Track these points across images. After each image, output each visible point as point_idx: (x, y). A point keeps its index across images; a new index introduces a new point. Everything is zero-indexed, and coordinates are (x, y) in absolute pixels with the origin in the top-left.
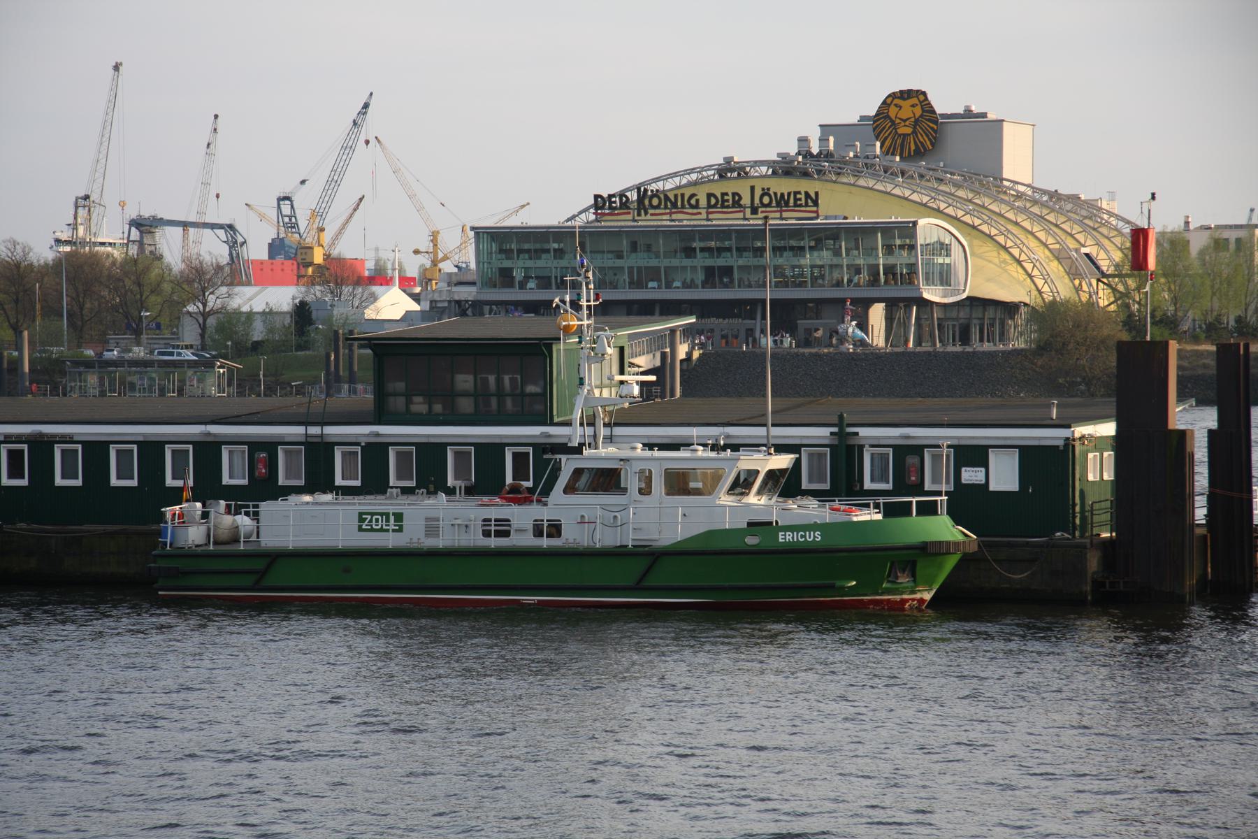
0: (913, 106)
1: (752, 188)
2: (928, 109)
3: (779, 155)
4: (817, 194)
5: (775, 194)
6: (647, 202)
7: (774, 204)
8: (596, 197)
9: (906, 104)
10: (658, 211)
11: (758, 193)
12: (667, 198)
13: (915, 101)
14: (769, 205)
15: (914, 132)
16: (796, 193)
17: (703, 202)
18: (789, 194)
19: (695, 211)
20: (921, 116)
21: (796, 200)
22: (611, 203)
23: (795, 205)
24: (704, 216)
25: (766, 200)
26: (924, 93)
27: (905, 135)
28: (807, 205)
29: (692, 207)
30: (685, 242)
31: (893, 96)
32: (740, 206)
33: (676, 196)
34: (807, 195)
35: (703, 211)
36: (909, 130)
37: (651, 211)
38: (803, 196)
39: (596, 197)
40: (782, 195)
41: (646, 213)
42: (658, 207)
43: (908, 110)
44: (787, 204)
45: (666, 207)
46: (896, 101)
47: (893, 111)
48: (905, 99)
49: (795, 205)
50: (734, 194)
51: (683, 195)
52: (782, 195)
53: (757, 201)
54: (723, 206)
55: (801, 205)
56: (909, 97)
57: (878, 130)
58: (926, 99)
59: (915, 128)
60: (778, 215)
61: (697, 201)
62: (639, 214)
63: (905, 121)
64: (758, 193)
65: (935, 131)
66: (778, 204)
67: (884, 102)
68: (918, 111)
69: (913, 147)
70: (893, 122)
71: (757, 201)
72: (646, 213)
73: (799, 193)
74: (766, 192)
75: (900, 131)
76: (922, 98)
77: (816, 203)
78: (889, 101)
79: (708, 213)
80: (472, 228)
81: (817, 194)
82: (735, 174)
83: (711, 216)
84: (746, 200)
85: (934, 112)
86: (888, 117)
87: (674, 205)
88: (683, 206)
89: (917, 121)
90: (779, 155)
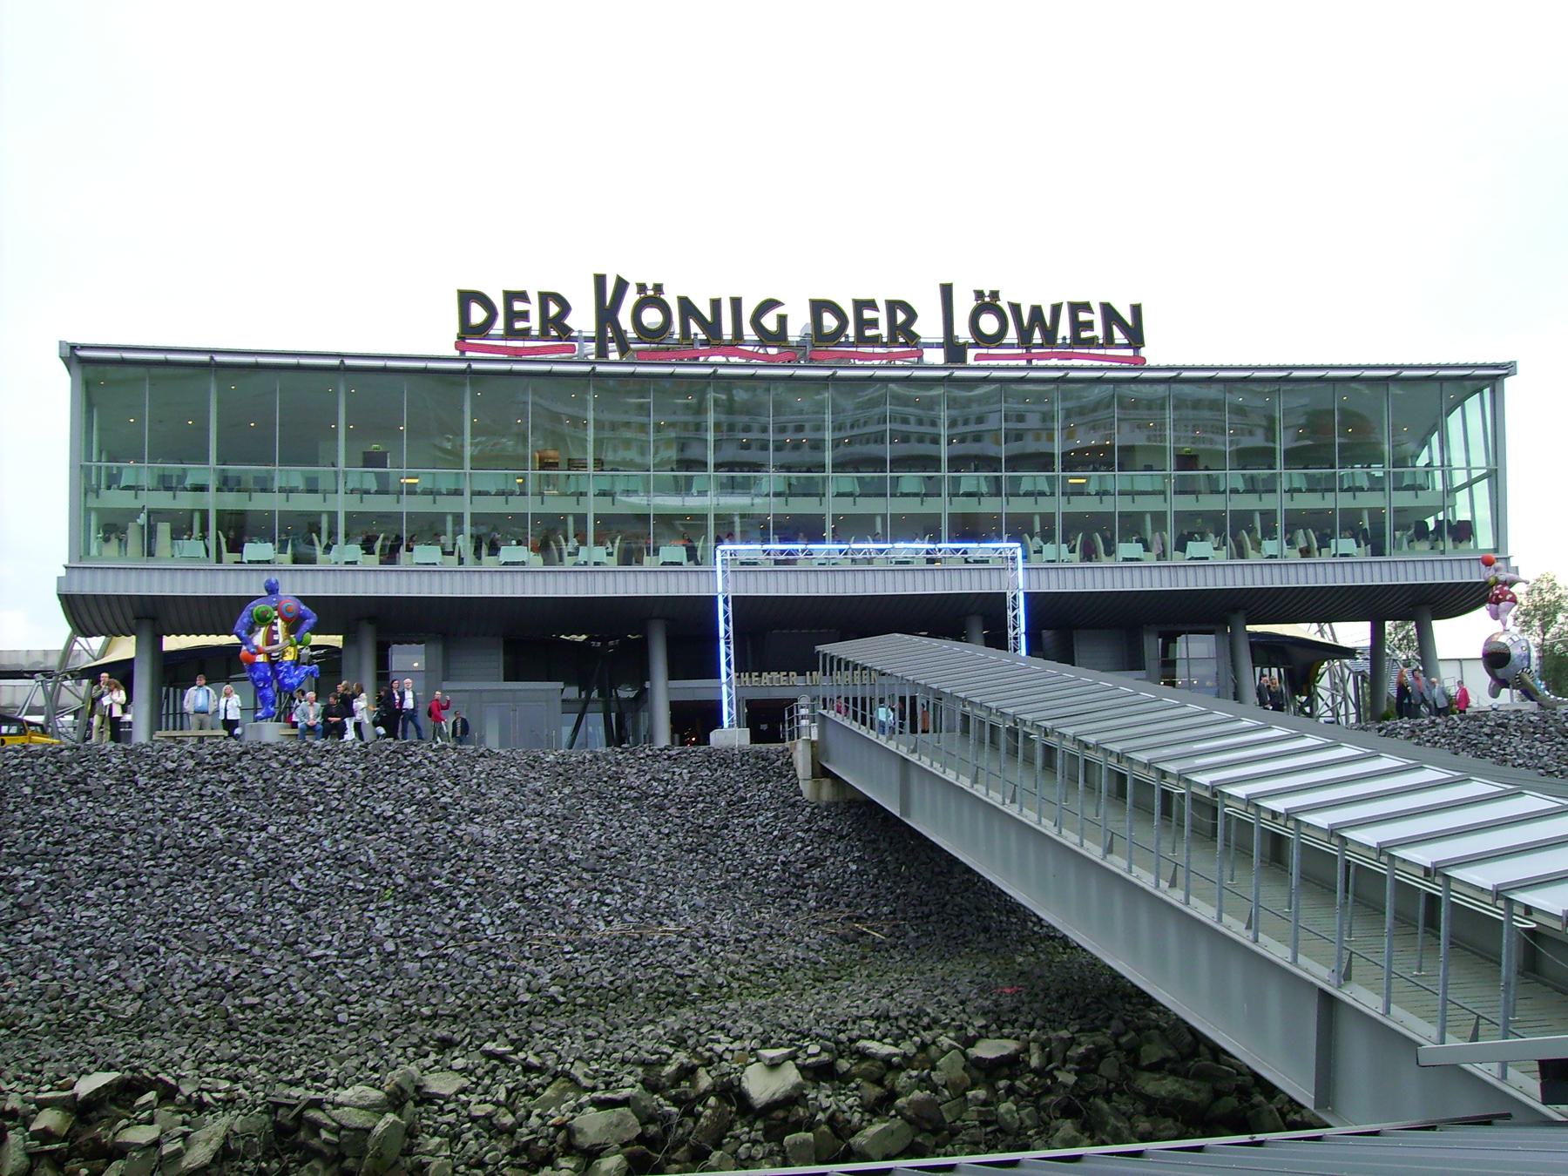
1: (947, 291)
4: (1136, 310)
5: (1016, 308)
6: (625, 318)
7: (1012, 335)
8: (467, 298)
16: (1076, 308)
18: (1056, 309)
21: (1077, 326)
25: (989, 324)
33: (716, 304)
34: (1109, 313)
38: (1097, 318)
39: (467, 298)
40: (1036, 311)
44: (1050, 335)
49: (1077, 341)
50: (893, 306)
51: (736, 303)
52: (1036, 311)
53: (962, 332)
61: (782, 320)
71: (962, 332)
73: (1086, 307)
77: (1136, 337)
80: (74, 357)
81: (1136, 310)
84: (929, 327)
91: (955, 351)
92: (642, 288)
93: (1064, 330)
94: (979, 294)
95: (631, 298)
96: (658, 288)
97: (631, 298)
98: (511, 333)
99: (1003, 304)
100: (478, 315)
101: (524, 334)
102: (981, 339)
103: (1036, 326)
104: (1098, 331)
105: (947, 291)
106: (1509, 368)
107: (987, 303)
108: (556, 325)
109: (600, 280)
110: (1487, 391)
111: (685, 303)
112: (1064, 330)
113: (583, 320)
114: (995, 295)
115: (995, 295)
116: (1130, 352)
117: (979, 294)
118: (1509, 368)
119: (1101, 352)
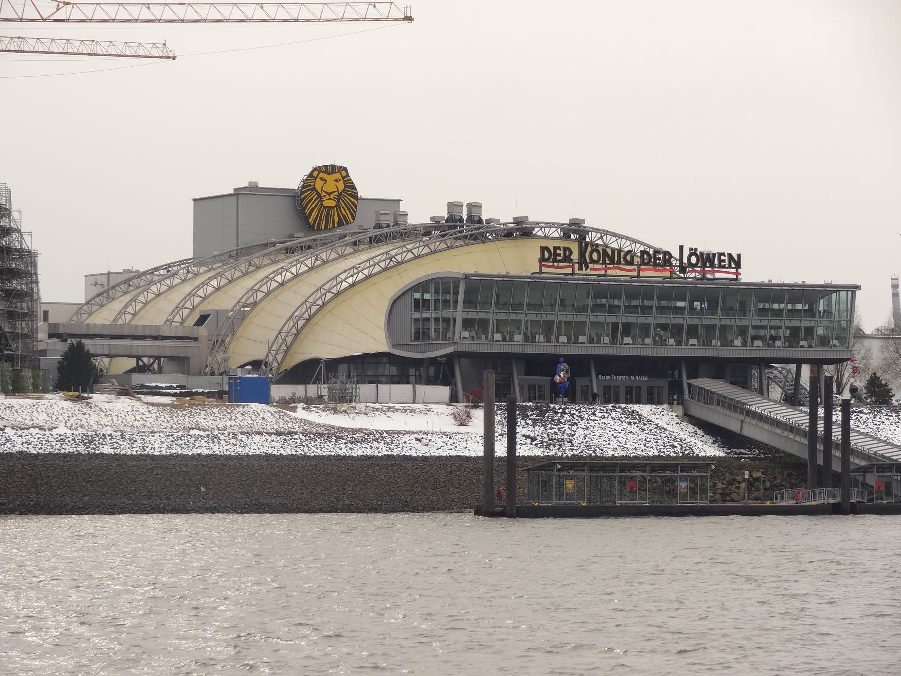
0: (336, 181)
1: (681, 248)
2: (350, 187)
3: (432, 219)
4: (739, 256)
9: (330, 178)
10: (596, 266)
12: (604, 251)
13: (338, 176)
15: (338, 205)
16: (721, 255)
17: (637, 260)
19: (628, 267)
20: (344, 191)
21: (720, 261)
22: (556, 255)
23: (720, 266)
26: (346, 169)
27: (330, 208)
28: (730, 267)
29: (627, 263)
34: (730, 256)
36: (333, 204)
37: (591, 266)
38: (726, 258)
41: (587, 268)
42: (596, 262)
43: (332, 185)
45: (604, 263)
46: (322, 175)
47: (319, 185)
48: (329, 174)
53: (685, 261)
54: (655, 264)
55: (724, 267)
56: (333, 172)
58: (348, 175)
59: (338, 202)
62: (580, 269)
63: (329, 194)
66: (704, 266)
67: (311, 175)
68: (341, 186)
69: (337, 220)
70: (319, 195)
71: (685, 261)
72: (587, 268)
73: (724, 254)
74: (693, 252)
75: (326, 203)
76: (344, 173)
77: (738, 265)
78: (315, 174)
85: (354, 188)
86: (314, 189)
88: (619, 263)
89: (340, 195)
90: (432, 219)
91: (683, 270)
93: (716, 262)
94: (691, 249)
95: (589, 249)
98: (555, 261)
99: (698, 253)
100: (546, 255)
102: (690, 264)
103: (707, 260)
104: (727, 263)
105: (681, 248)
106: (858, 288)
107: (693, 252)
108: (567, 259)
110: (850, 293)
112: (716, 262)
113: (575, 257)
114: (696, 249)
115: (696, 249)
116: (734, 271)
117: (691, 249)
118: (858, 288)
119: (726, 270)
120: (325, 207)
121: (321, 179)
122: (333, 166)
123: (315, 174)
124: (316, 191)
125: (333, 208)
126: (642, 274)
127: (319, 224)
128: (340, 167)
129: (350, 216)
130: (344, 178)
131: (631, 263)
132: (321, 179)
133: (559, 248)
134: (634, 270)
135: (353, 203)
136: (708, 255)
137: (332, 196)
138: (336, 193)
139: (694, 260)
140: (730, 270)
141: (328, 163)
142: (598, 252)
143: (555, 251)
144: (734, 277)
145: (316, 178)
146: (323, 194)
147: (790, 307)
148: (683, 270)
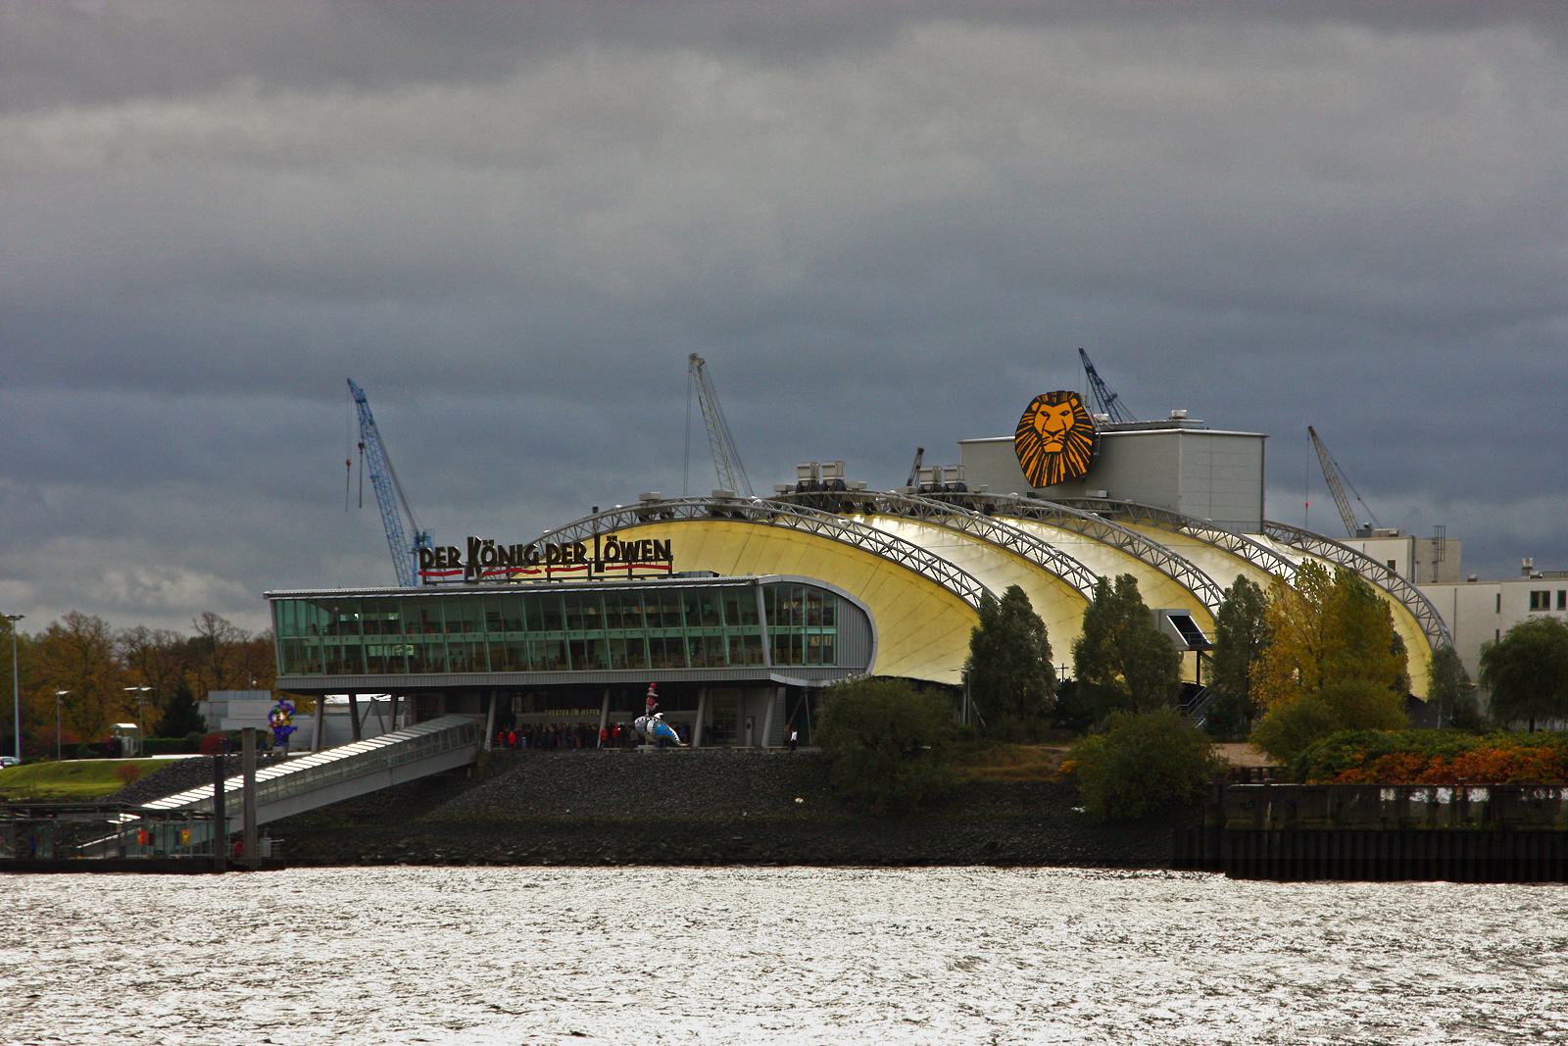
4: (668, 543)
11: (604, 542)
13: (1065, 407)
14: (615, 559)
15: (1065, 450)
16: (646, 542)
18: (637, 543)
19: (533, 568)
20: (1073, 428)
21: (645, 551)
23: (645, 559)
24: (544, 575)
26: (1077, 396)
27: (1054, 454)
28: (657, 559)
30: (547, 608)
31: (1039, 400)
32: (585, 561)
33: (512, 548)
35: (543, 568)
36: (1058, 447)
43: (1058, 420)
46: (1044, 408)
47: (1039, 422)
48: (1053, 405)
49: (645, 559)
56: (1059, 402)
57: (1021, 448)
58: (1080, 404)
59: (1065, 444)
60: (626, 572)
61: (536, 554)
63: (1053, 434)
64: (604, 542)
65: (1092, 449)
67: (1029, 409)
68: (1069, 420)
69: (1063, 471)
70: (1039, 436)
73: (648, 542)
75: (1048, 449)
76: (1074, 402)
77: (668, 557)
79: (549, 571)
82: (658, 518)
83: (553, 575)
84: (590, 554)
86: (1033, 429)
87: (511, 560)
89: (1068, 435)
92: (485, 542)
95: (482, 547)
96: (492, 542)
97: (482, 547)
98: (439, 566)
101: (444, 566)
109: (470, 540)
111: (500, 547)
112: (640, 554)
113: (463, 560)
116: (666, 563)
119: (653, 563)
120: (1047, 454)
121: (1043, 413)
122: (1060, 394)
123: (1035, 407)
124: (1036, 432)
125: (1058, 453)
126: (553, 575)
127: (1039, 478)
128: (1070, 393)
129: (1081, 464)
130: (1073, 409)
131: (535, 562)
132: (1043, 413)
133: (442, 549)
134: (540, 572)
135: (1086, 444)
136: (630, 544)
137: (1056, 438)
138: (1063, 433)
139: (612, 552)
140: (660, 563)
141: (1054, 389)
142: (493, 551)
143: (564, 549)
144: (666, 572)
145: (1035, 413)
146: (1045, 435)
147: (665, 609)
148: (600, 568)
